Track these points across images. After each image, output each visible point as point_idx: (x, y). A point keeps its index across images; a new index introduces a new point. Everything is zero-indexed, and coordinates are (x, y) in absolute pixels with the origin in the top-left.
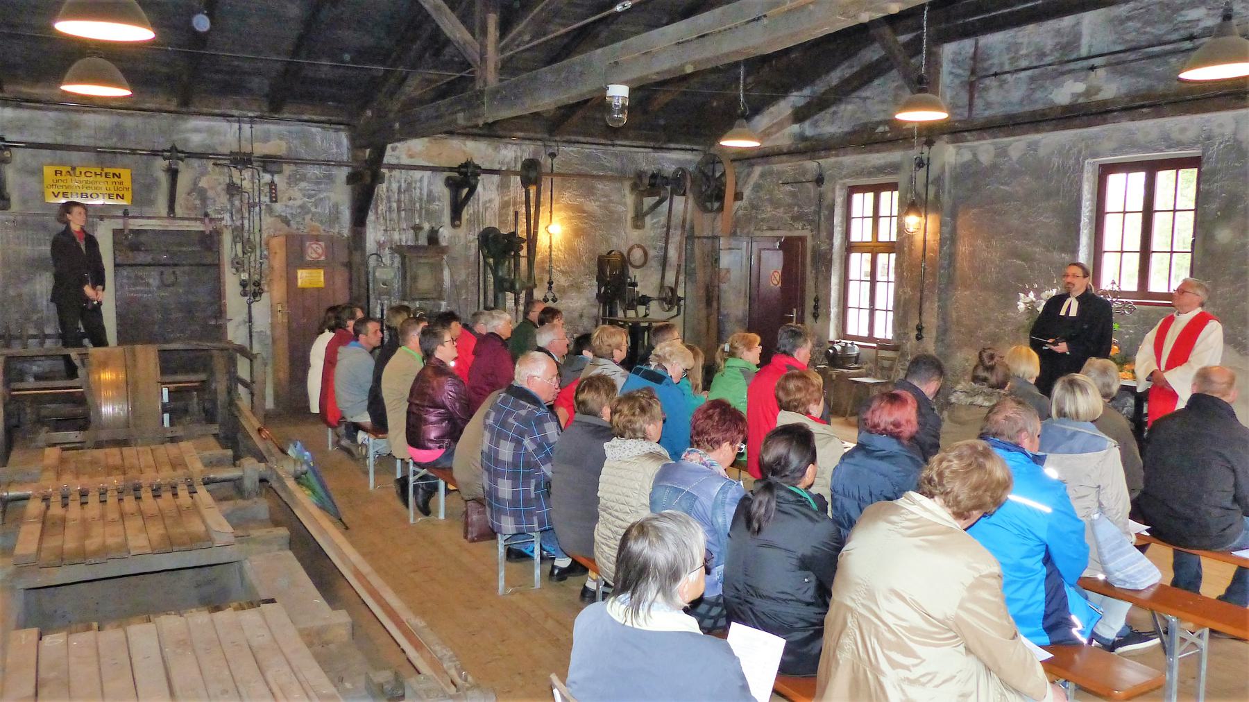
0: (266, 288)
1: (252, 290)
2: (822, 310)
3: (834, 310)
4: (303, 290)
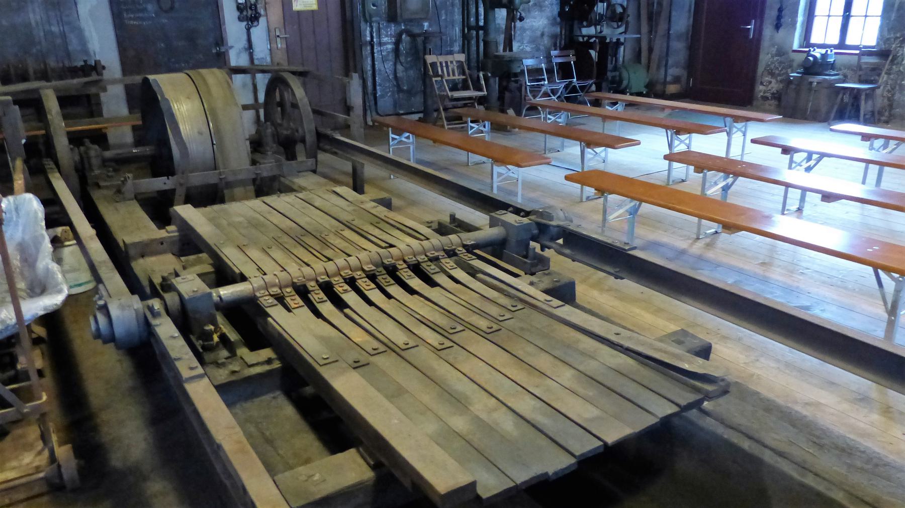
0: (262, 12)
1: (250, 15)
2: (786, 20)
3: (800, 18)
4: (299, 12)
